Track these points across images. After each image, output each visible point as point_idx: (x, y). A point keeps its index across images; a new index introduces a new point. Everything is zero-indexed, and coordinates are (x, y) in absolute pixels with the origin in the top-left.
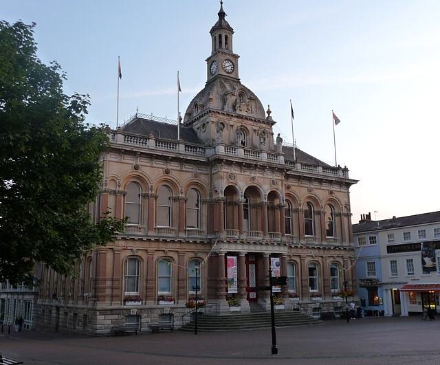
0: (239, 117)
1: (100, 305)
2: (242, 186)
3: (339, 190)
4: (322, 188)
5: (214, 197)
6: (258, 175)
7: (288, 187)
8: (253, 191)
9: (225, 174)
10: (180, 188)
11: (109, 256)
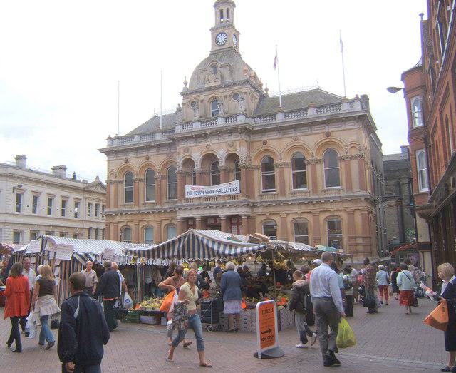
2: (197, 157)
4: (314, 132)
6: (213, 142)
8: (210, 158)
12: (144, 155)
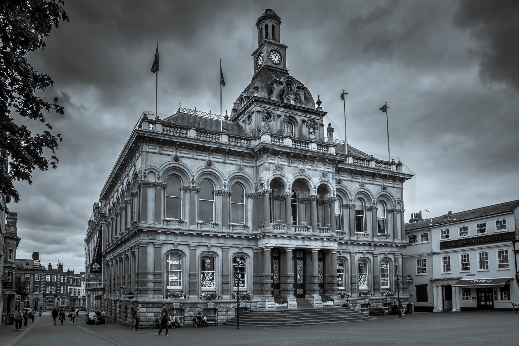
0: (288, 107)
1: (141, 299)
3: (392, 185)
4: (375, 183)
5: (259, 191)
7: (339, 182)
9: (271, 165)
10: (223, 182)
11: (151, 250)
12: (206, 158)
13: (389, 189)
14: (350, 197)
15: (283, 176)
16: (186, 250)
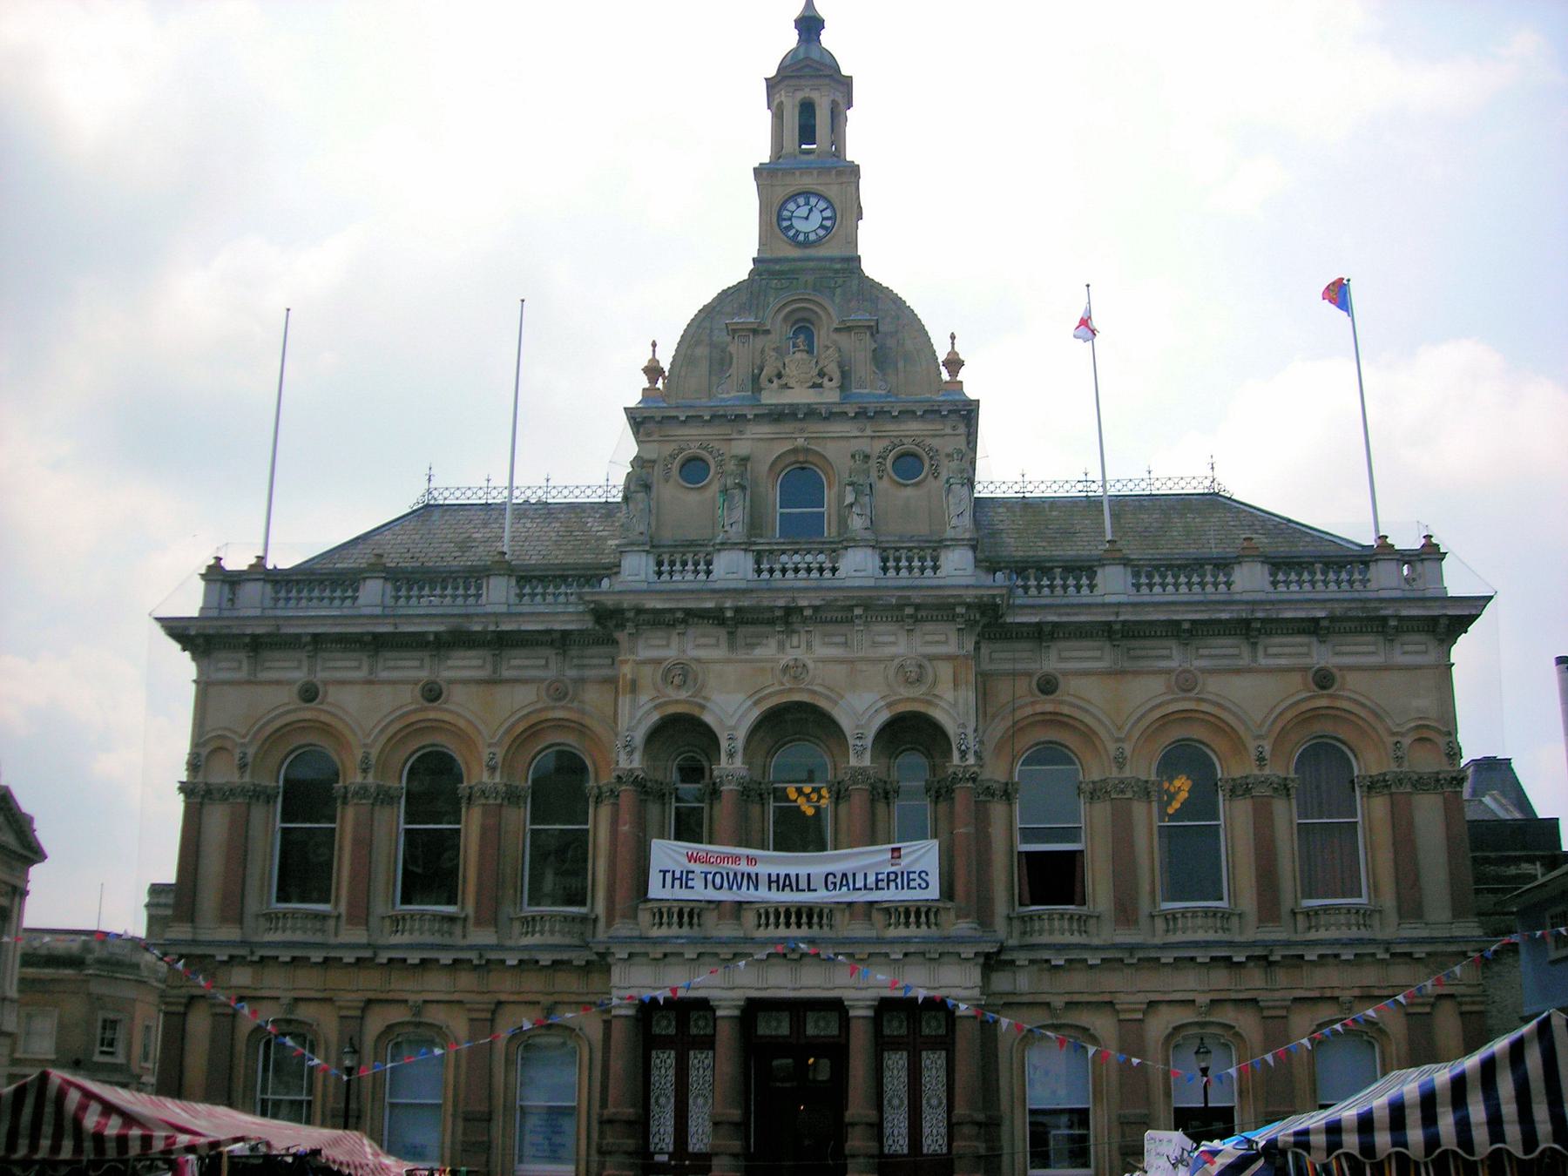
4: (1263, 661)
6: (822, 651)
9: (647, 670)
13: (1354, 684)
14: (1112, 747)
15: (703, 707)
16: (327, 1023)
